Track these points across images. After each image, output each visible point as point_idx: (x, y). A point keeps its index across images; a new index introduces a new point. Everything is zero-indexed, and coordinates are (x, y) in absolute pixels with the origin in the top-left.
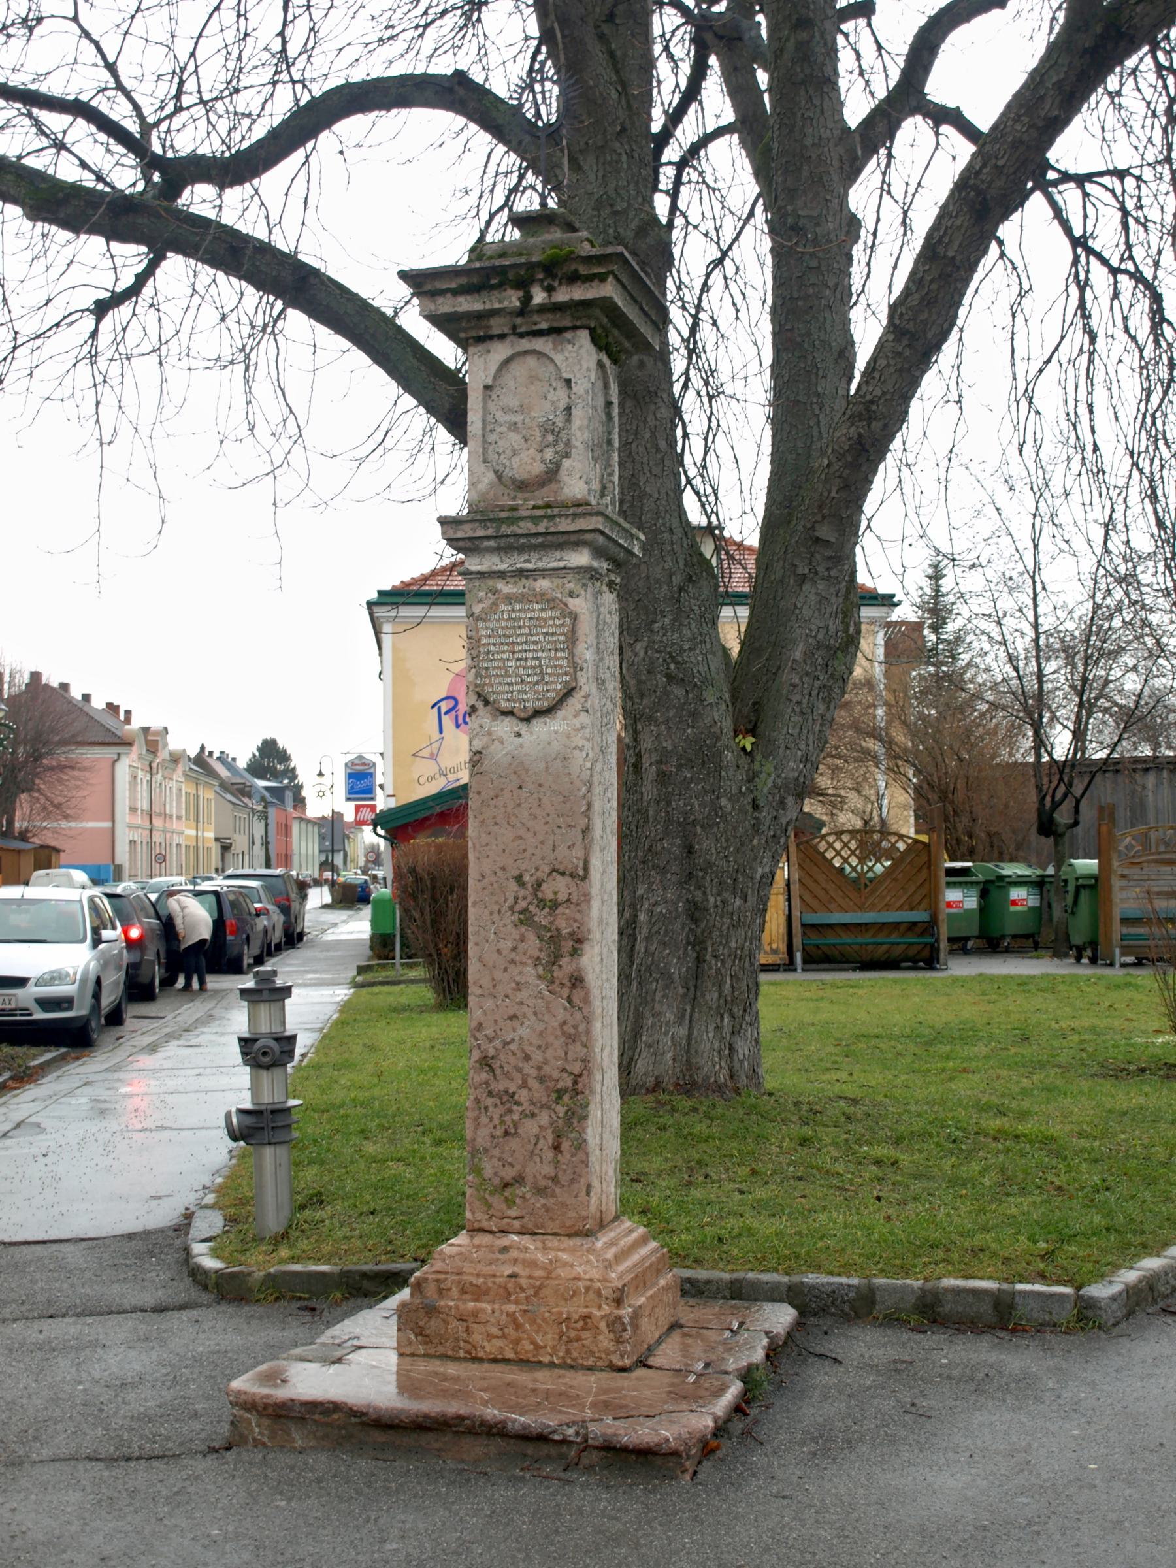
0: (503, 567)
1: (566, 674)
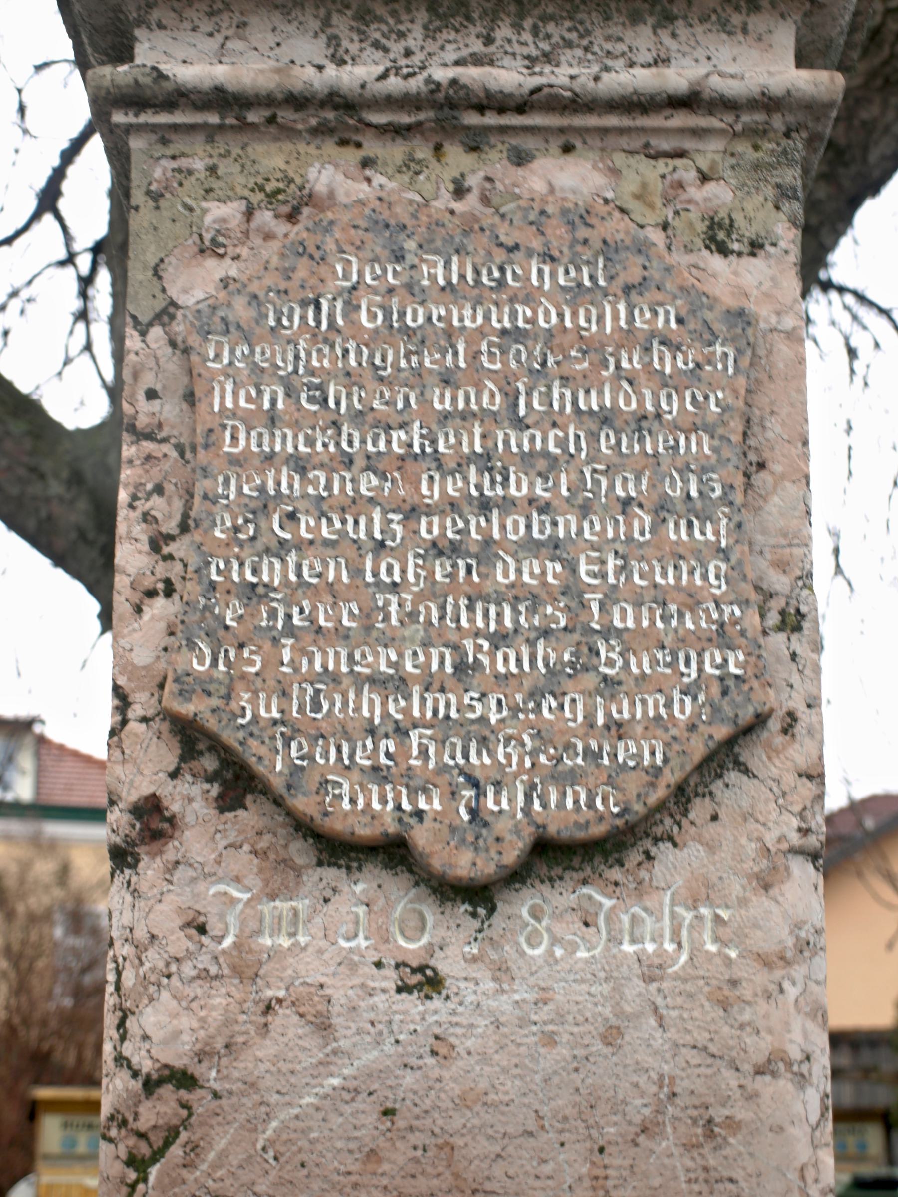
0: (360, 73)
1: (722, 636)
